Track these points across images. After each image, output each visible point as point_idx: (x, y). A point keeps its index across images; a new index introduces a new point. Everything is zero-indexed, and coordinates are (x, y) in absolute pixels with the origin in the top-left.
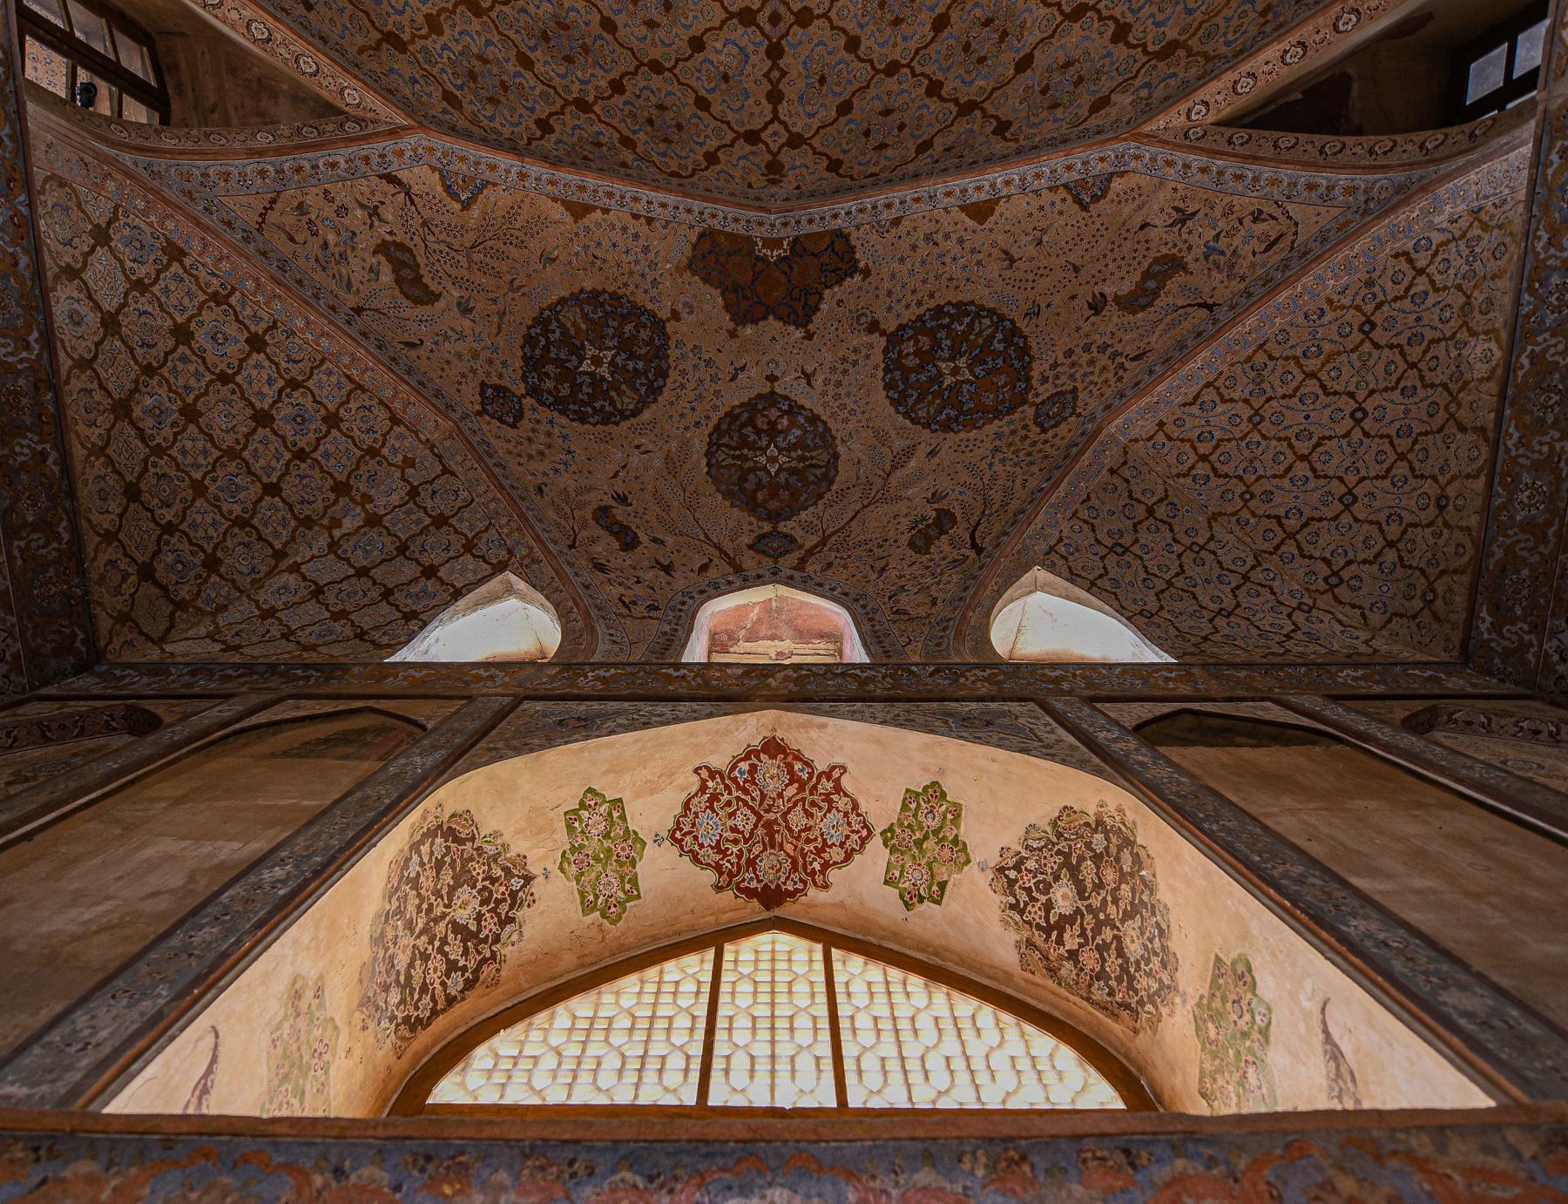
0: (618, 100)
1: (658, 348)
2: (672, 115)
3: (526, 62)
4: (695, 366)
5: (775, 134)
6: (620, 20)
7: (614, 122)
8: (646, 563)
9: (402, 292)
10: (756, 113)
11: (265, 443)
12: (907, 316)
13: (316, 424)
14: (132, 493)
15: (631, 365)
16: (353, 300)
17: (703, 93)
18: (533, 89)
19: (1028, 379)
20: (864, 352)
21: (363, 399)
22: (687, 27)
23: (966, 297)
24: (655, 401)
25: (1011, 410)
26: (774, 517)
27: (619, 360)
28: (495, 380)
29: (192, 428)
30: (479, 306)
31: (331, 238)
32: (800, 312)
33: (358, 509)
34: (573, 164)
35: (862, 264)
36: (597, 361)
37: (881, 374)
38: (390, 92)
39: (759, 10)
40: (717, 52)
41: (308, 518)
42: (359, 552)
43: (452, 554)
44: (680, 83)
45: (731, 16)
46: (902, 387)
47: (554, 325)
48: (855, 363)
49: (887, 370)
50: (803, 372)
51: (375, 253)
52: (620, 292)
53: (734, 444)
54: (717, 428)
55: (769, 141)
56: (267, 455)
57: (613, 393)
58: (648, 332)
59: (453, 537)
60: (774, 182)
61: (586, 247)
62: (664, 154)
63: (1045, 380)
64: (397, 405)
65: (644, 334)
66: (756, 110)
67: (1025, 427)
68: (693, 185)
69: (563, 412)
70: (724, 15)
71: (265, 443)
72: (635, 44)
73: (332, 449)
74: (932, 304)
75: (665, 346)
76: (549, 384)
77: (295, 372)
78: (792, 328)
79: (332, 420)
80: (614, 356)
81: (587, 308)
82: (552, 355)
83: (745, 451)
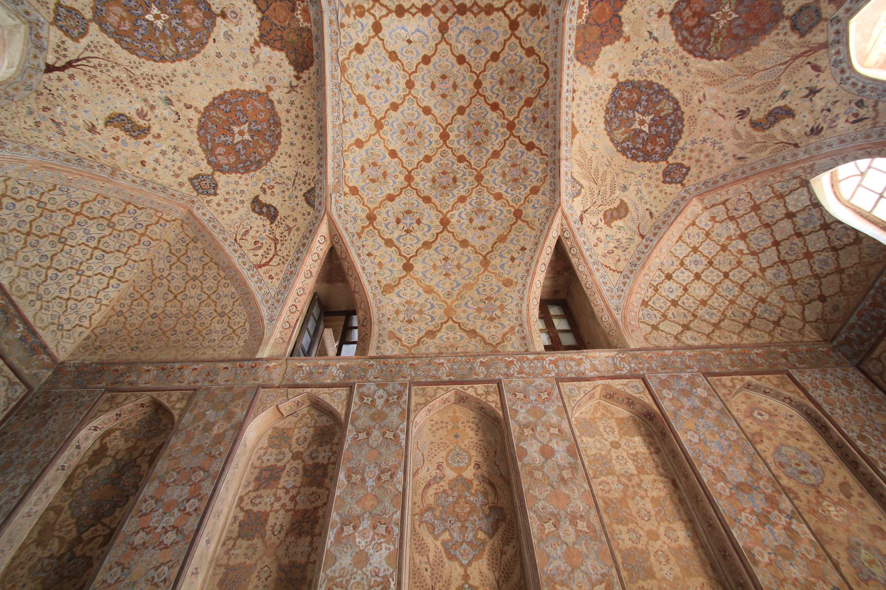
0: (503, 106)
2: (505, 75)
3: (496, 154)
4: (646, 64)
5: (512, 9)
6: (457, 105)
7: (517, 109)
9: (625, 216)
10: (499, 22)
11: (707, 277)
13: (697, 256)
14: (747, 325)
15: (644, 103)
16: (638, 239)
17: (488, 56)
18: (510, 152)
21: (685, 236)
22: (453, 66)
24: (667, 90)
27: (641, 110)
28: (660, 176)
29: (709, 302)
30: (621, 181)
31: (611, 245)
33: (734, 242)
34: (555, 133)
36: (642, 123)
38: (547, 218)
39: (440, 20)
40: (463, 47)
41: (738, 262)
42: (761, 244)
43: (781, 205)
44: (484, 71)
45: (443, 38)
47: (625, 145)
53: (705, 41)
54: (690, 52)
55: (516, 14)
56: (713, 276)
60: (544, 11)
62: (533, 81)
64: (687, 223)
65: (626, 95)
66: (497, 22)
69: (676, 142)
70: (444, 43)
71: (707, 277)
72: (468, 96)
73: (707, 251)
75: (632, 82)
76: (658, 149)
77: (677, 263)
79: (695, 250)
81: (614, 127)
83: (712, 34)
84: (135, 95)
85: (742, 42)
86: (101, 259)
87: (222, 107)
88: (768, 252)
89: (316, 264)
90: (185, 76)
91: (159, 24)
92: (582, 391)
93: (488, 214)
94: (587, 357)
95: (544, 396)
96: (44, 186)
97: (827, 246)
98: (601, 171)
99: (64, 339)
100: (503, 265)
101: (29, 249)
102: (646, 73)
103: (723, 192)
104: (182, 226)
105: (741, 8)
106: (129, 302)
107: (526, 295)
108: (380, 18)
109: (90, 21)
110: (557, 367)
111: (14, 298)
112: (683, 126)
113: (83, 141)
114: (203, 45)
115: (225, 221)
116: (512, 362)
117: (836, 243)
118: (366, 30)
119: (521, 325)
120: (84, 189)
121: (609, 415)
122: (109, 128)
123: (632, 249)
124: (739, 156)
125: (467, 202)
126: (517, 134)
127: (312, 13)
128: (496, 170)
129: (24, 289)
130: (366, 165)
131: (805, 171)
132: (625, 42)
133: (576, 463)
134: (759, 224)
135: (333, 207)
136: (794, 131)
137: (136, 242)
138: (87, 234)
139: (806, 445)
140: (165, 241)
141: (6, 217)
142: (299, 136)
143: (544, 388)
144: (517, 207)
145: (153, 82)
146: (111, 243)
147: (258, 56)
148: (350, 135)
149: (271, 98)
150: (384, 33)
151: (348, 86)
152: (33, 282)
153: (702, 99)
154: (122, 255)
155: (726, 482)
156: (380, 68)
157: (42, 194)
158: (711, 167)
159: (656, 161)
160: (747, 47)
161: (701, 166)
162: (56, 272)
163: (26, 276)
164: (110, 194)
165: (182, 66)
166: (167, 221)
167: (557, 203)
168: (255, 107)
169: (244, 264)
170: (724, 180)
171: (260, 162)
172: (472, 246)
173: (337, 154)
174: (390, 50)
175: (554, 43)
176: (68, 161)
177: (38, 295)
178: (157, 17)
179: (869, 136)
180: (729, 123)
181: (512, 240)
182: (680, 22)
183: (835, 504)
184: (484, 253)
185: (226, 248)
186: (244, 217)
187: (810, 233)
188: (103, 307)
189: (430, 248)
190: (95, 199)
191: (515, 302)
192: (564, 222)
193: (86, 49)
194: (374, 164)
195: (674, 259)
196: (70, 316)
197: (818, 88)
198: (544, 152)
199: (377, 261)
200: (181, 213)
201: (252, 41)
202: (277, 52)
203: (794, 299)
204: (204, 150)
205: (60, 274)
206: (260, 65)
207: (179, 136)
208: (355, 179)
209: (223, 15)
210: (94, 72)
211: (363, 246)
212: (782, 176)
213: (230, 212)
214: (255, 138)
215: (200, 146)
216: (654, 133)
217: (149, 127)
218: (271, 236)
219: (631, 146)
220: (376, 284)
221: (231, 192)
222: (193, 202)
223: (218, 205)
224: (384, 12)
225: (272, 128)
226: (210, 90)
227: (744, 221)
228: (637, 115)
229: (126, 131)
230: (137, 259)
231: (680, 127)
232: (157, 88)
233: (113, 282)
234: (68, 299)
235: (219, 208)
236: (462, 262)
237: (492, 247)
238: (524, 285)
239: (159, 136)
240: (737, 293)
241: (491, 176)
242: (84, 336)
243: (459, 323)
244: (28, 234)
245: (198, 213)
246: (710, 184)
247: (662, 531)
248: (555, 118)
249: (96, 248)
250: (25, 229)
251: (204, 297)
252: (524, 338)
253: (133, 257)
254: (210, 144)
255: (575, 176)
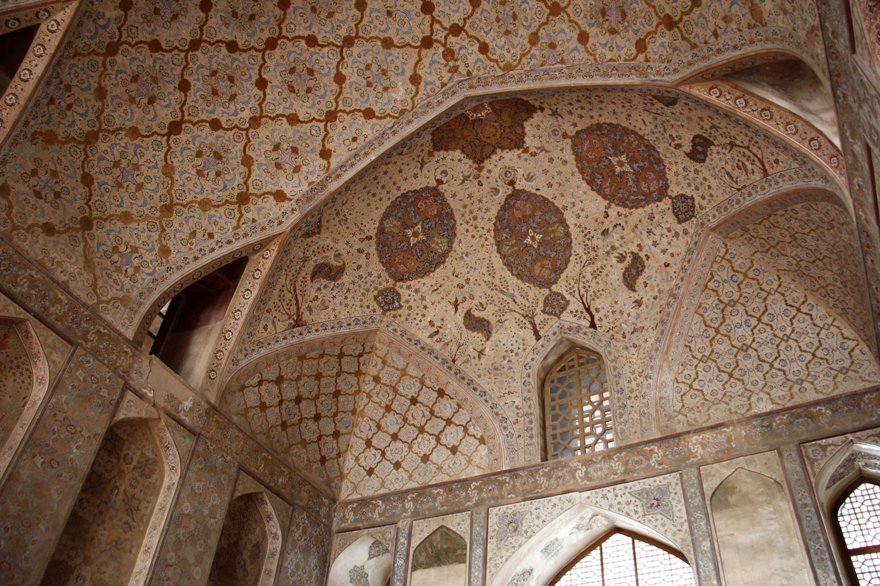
84: (605, 262)
86: (773, 317)
87: (599, 182)
89: (751, 103)
90: (578, 216)
91: (538, 237)
96: (686, 355)
99: (860, 371)
101: (746, 378)
104: (731, 238)
106: (830, 300)
108: (445, 29)
109: (550, 290)
111: (789, 405)
113: (648, 313)
114: (545, 199)
115: (720, 196)
118: (463, 43)
120: (690, 324)
122: (637, 288)
127: (473, 104)
129: (783, 393)
130: (606, 25)
135: (665, 78)
137: (755, 282)
138: (741, 325)
140: (753, 255)
141: (711, 389)
142: (603, 106)
145: (589, 243)
146: (754, 305)
147: (538, 149)
148: (575, 53)
149: (574, 133)
150: (456, 19)
151: (524, 59)
152: (780, 383)
154: (770, 297)
156: (494, 16)
157: (693, 357)
162: (778, 360)
163: (772, 388)
164: (695, 302)
165: (570, 219)
166: (727, 252)
168: (589, 150)
169: (763, 188)
171: (647, 146)
173: (602, 70)
174: (471, 8)
176: (662, 332)
177: (796, 382)
178: (533, 238)
185: (746, 203)
186: (712, 172)
188: (836, 323)
190: (702, 316)
193: (574, 296)
194: (603, 13)
196: (835, 358)
199: (722, 24)
200: (716, 241)
201: (525, 156)
202: (527, 130)
204: (648, 204)
205: (782, 357)
206: (546, 146)
207: (636, 226)
208: (625, 44)
209: (512, 183)
210: (591, 293)
211: (706, 43)
213: (709, 187)
214: (622, 150)
215: (643, 207)
217: (632, 253)
218: (728, 148)
220: (754, 31)
221: (688, 181)
222: (702, 224)
223: (703, 198)
224: (437, 26)
225: (606, 132)
226: (585, 193)
229: (639, 273)
230: (776, 284)
232: (595, 242)
233: (804, 309)
234: (814, 355)
235: (707, 198)
239: (639, 245)
242: (866, 350)
244: (731, 375)
245: (713, 223)
249: (759, 320)
250: (725, 377)
251: (813, 233)
253: (775, 286)
254: (640, 197)
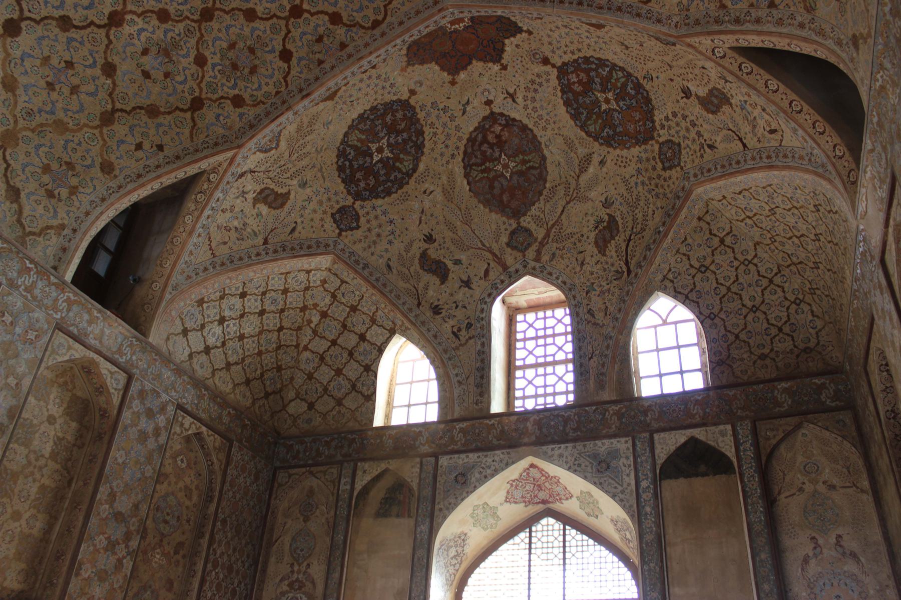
1: (411, 118)
7: (320, 8)
8: (457, 285)
9: (275, 209)
11: (268, 318)
12: (567, 58)
13: (280, 298)
15: (400, 139)
16: (260, 240)
18: (264, 32)
19: (653, 122)
20: (544, 77)
21: (293, 275)
23: (603, 57)
24: (423, 153)
25: (645, 142)
26: (517, 214)
27: (392, 140)
29: (245, 340)
30: (309, 175)
31: (236, 223)
32: (494, 54)
33: (315, 311)
34: (317, 79)
35: (525, 28)
36: (380, 150)
37: (559, 94)
42: (327, 332)
43: (367, 326)
46: (575, 106)
48: (541, 85)
49: (562, 91)
50: (508, 93)
51: (254, 207)
52: (375, 104)
53: (479, 161)
54: (465, 153)
57: (398, 164)
58: (401, 113)
59: (364, 316)
61: (344, 103)
63: (663, 127)
64: (306, 267)
65: (399, 115)
67: (654, 159)
68: (391, 24)
69: (377, 197)
73: (291, 300)
74: (581, 55)
75: (415, 113)
76: (362, 184)
78: (490, 65)
80: (389, 139)
81: (361, 126)
82: (356, 166)
85: (489, 196)
88: (323, 342)
92: (69, 354)
93: (170, 67)
94: (104, 319)
95: (32, 335)
97: (354, 380)
98: (308, 148)
100: (123, 142)
102: (429, 122)
103: (352, 275)
105: (515, 178)
107: (112, 199)
110: (69, 310)
112: (396, 192)
116: (30, 269)
117: (359, 385)
119: (75, 231)
121: (70, 387)
123: (246, 244)
124: (391, 263)
125: (164, 26)
126: (291, 27)
128: (233, 30)
131: (401, 326)
132: (450, 82)
133: (7, 426)
134: (342, 320)
136: (431, 293)
139: (187, 503)
143: (38, 326)
144: (203, 96)
153: (428, 192)
155: (111, 507)
158: (370, 247)
159: (349, 193)
160: (486, 203)
161: (366, 237)
167: (240, 142)
170: (363, 268)
172: (114, 83)
175: (413, 12)
179: (445, 351)
180: (416, 233)
181: (160, 125)
182: (487, 126)
183: (163, 554)
184: (118, 106)
187: (357, 361)
189: (65, 30)
191: (93, 198)
192: (225, 165)
195: (264, 284)
197: (472, 286)
198: (289, 79)
203: (297, 387)
212: (389, 313)
216: (376, 169)
219: (350, 157)
227: (337, 307)
228: (385, 141)
231: (394, 190)
236: (83, 89)
237: (134, 108)
238: (120, 187)
240: (270, 349)
241: (219, 30)
243: (8, 165)
246: (353, 258)
247: (27, 516)
248: (333, 67)
252: (64, 250)
255: (285, 133)
